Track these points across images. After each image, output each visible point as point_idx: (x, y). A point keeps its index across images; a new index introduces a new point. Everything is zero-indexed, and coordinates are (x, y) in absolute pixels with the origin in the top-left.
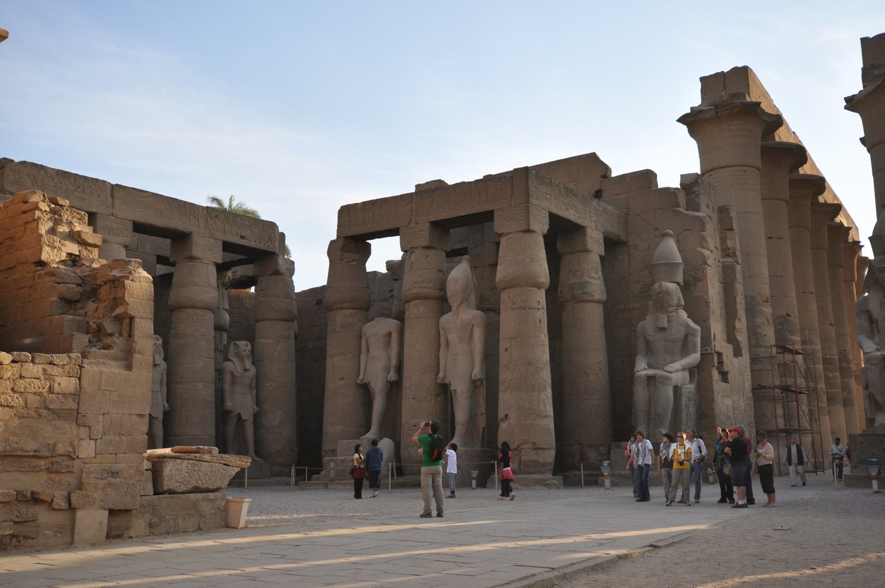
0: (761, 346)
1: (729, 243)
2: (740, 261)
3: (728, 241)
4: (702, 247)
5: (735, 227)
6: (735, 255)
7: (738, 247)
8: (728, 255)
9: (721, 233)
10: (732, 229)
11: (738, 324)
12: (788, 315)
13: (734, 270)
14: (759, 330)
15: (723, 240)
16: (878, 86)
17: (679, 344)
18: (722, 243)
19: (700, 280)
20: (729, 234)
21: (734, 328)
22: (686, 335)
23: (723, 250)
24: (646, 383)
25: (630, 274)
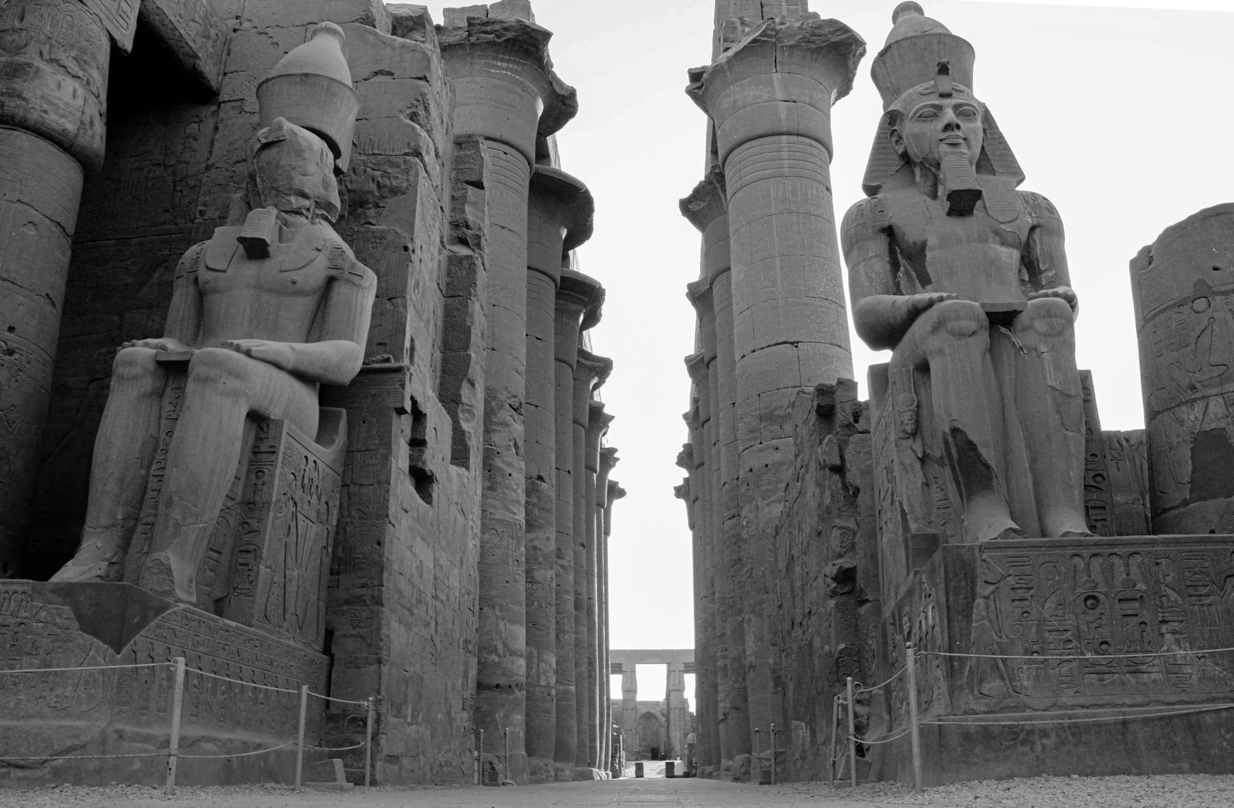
1: (470, 214)
3: (467, 208)
4: (414, 117)
6: (478, 245)
8: (463, 241)
9: (454, 189)
10: (479, 185)
12: (540, 478)
15: (458, 201)
16: (755, 41)
17: (304, 305)
19: (394, 191)
20: (471, 190)
22: (331, 281)
23: (455, 225)
24: (148, 383)
25: (207, 168)
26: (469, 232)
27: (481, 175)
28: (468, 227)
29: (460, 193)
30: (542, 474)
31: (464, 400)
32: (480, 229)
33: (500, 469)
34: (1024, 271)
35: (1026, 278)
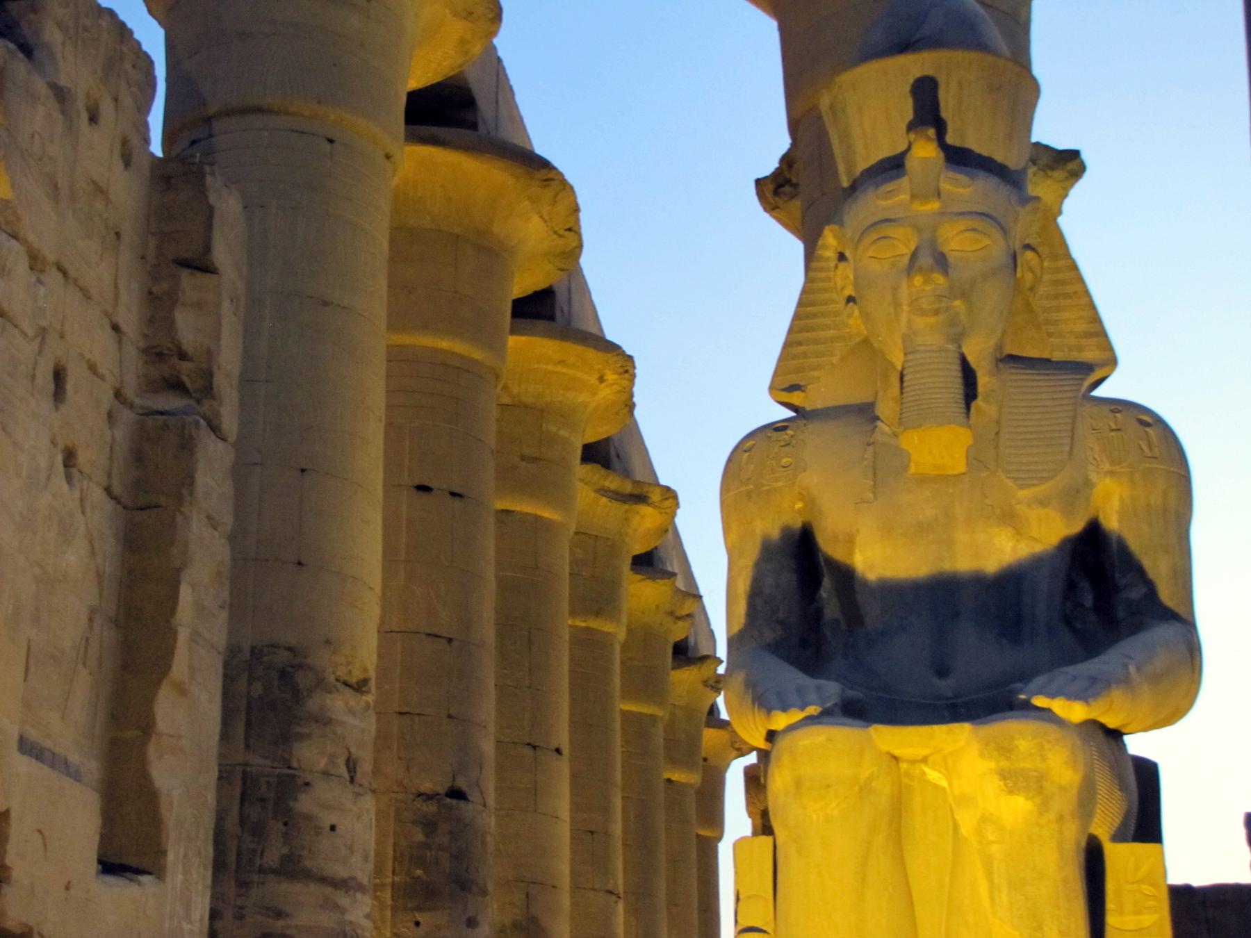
0: (307, 875)
1: (188, 328)
2: (230, 422)
5: (221, 256)
6: (208, 390)
7: (229, 360)
8: (177, 386)
9: (155, 276)
10: (202, 265)
11: (168, 711)
13: (187, 445)
14: (304, 803)
15: (159, 306)
18: (151, 321)
20: (187, 279)
21: (147, 727)
23: (154, 354)
26: (185, 366)
27: (207, 249)
28: (183, 356)
29: (165, 286)
30: (461, 783)
31: (162, 724)
32: (210, 355)
33: (309, 818)
34: (1085, 586)
35: (1089, 601)
